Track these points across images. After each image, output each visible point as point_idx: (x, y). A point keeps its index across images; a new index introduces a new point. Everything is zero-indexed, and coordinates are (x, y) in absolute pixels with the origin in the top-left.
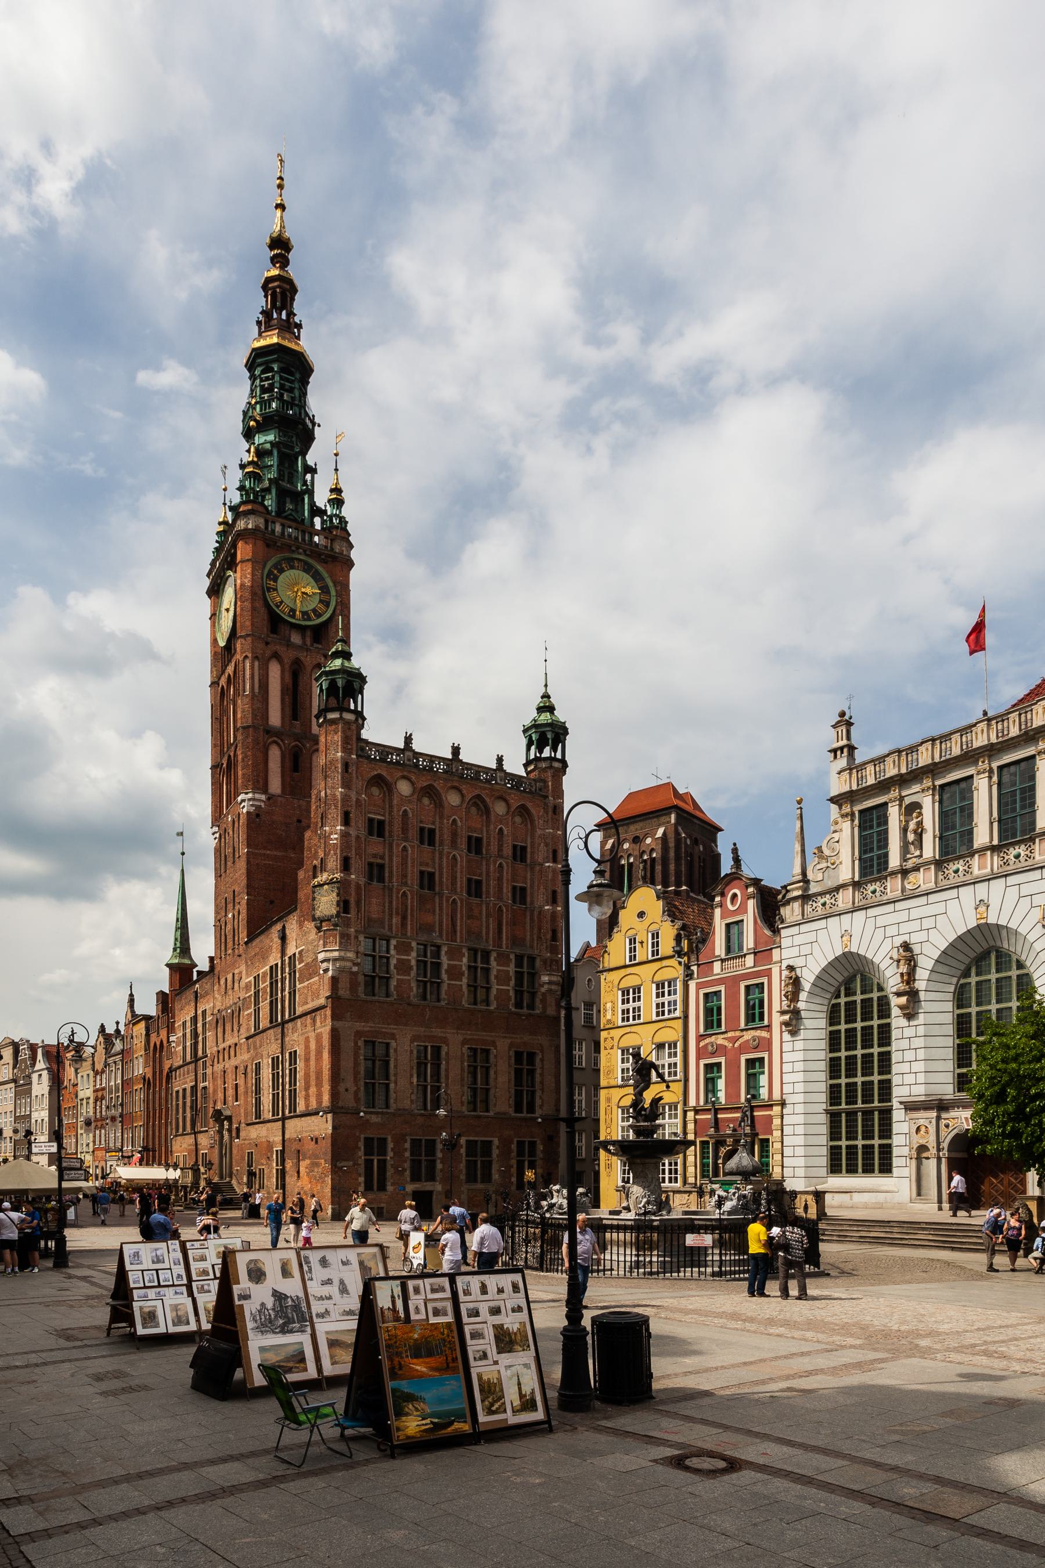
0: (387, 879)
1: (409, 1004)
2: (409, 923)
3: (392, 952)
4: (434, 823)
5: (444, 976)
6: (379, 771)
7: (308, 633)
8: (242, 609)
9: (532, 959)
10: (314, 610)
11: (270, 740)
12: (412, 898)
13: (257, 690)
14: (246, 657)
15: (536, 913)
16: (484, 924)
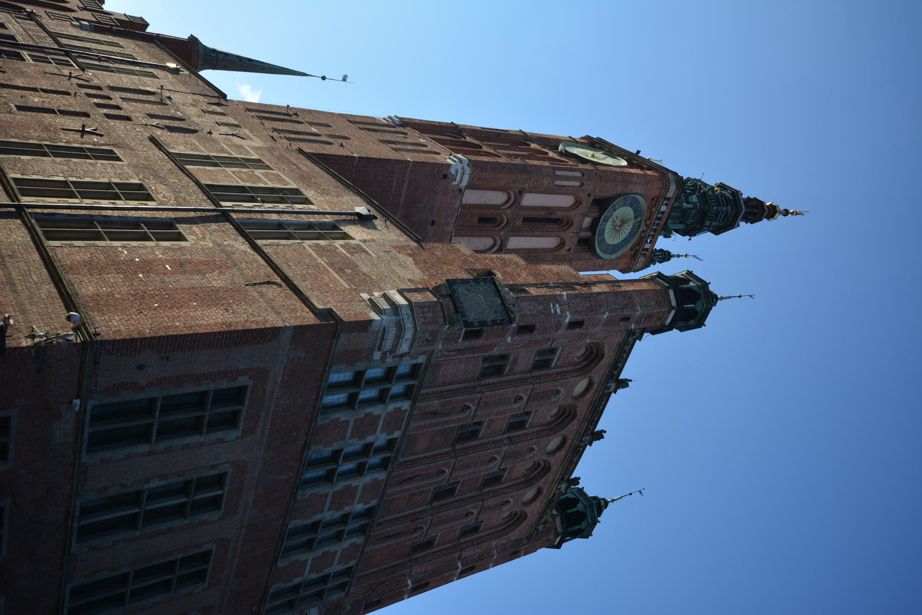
0: (486, 381)
1: (306, 446)
2: (428, 422)
3: (391, 407)
4: (531, 426)
5: (340, 486)
6: (606, 356)
7: (589, 234)
8: (616, 172)
9: (342, 587)
10: (604, 240)
11: (512, 194)
12: (459, 420)
13: (558, 183)
14: (583, 175)
15: (403, 572)
16: (400, 515)
